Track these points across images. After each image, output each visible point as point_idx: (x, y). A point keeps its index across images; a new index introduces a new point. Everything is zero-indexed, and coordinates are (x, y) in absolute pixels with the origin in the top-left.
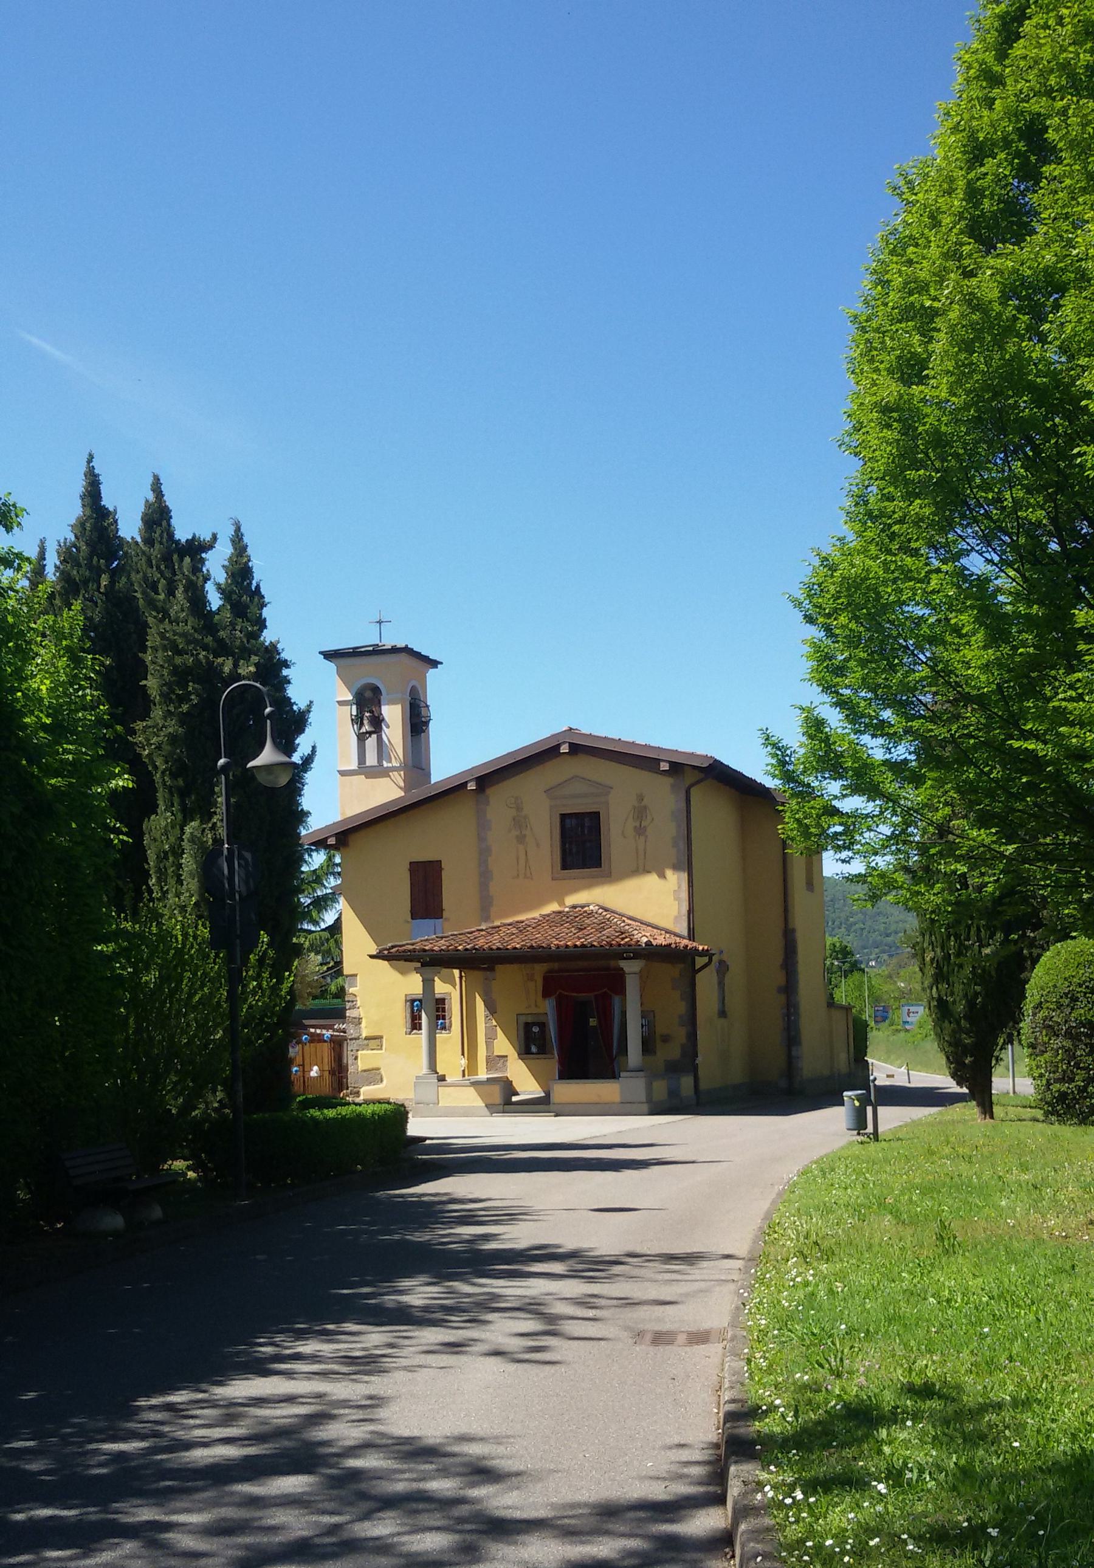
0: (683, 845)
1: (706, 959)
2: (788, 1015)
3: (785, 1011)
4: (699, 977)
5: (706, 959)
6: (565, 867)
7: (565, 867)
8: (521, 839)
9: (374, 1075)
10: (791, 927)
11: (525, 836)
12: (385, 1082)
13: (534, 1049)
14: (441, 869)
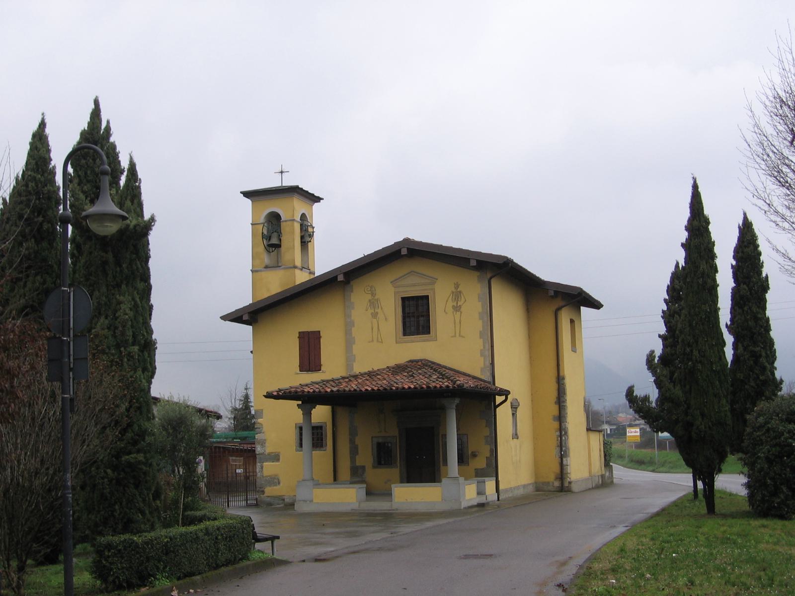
0: (487, 318)
1: (503, 398)
2: (561, 436)
3: (558, 433)
4: (498, 409)
5: (503, 398)
6: (405, 334)
7: (405, 334)
8: (375, 315)
9: (274, 481)
10: (561, 374)
11: (377, 313)
12: (281, 485)
13: (383, 462)
14: (320, 337)
